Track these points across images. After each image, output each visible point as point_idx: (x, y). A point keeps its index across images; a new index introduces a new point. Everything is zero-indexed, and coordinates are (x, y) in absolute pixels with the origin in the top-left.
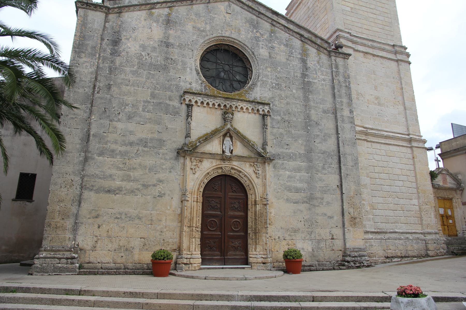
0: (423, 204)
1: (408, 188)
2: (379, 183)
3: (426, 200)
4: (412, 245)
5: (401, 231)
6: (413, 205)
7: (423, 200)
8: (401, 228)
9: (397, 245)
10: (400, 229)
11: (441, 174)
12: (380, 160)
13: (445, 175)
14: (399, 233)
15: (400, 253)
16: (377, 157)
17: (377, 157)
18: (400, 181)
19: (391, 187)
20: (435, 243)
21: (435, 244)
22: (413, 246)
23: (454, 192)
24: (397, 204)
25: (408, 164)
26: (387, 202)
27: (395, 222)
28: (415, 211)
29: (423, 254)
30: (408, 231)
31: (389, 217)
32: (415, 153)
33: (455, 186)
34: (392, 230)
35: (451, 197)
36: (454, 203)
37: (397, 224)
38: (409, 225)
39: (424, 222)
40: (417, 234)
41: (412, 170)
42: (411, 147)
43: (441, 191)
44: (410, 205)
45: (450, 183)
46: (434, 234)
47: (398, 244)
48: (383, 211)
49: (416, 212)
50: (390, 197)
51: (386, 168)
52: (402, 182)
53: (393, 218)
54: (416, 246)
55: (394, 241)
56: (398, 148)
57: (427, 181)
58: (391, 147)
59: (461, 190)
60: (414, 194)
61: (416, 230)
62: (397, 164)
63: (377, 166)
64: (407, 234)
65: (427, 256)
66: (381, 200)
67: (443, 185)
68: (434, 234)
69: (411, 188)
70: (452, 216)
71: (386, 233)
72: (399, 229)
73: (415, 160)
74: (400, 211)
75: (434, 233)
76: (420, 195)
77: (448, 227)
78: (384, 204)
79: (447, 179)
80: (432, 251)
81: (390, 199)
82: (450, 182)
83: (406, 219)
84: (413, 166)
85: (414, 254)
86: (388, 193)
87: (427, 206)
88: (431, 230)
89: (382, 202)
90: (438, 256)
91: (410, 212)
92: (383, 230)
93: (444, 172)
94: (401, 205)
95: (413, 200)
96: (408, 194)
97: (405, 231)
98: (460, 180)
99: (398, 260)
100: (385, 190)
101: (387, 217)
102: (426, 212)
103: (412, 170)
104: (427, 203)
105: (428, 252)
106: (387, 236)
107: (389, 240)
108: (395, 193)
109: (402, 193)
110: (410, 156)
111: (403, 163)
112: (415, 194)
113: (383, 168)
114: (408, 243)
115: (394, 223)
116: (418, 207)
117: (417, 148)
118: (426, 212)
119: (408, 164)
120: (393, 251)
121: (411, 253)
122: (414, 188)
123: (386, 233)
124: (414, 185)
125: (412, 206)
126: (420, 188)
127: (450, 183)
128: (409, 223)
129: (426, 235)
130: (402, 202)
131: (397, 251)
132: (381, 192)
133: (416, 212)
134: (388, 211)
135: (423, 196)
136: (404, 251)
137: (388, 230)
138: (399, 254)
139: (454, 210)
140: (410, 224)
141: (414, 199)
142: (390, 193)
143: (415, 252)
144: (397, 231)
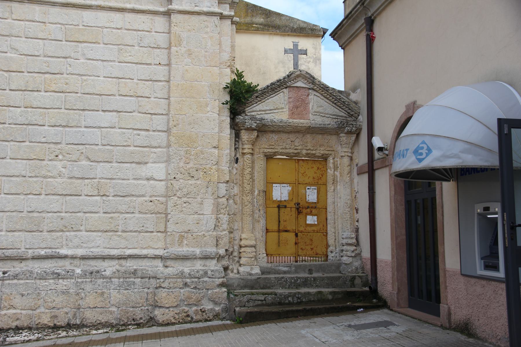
0: (178, 176)
1: (135, 132)
2: (21, 120)
3: (191, 165)
4: (103, 294)
5: (80, 252)
6: (148, 179)
7: (182, 164)
8: (85, 245)
9: (43, 293)
10: (82, 247)
11: (285, 90)
12: (36, 53)
13: (302, 90)
14: (73, 257)
15: (49, 315)
16: (23, 45)
17: (23, 45)
18: (107, 113)
19: (67, 129)
20: (186, 285)
21: (188, 289)
22: (105, 295)
23: (334, 137)
24: (82, 178)
25: (150, 64)
26: (44, 172)
27: (66, 227)
28: (151, 196)
29: (142, 315)
30: (107, 252)
31: (44, 215)
32: (174, 29)
33: (329, 122)
34: (43, 253)
35: (320, 151)
36: (329, 170)
37: (73, 233)
38: (119, 236)
39: (171, 227)
40: (146, 260)
41: (160, 81)
42: (168, 14)
43: (284, 136)
44: (135, 179)
45: (316, 114)
46: (200, 258)
47: (49, 292)
48: (22, 197)
49: (153, 199)
50: (60, 157)
51: (58, 76)
52: (115, 113)
53: (58, 217)
54: (116, 296)
55: (38, 281)
56: (117, 16)
57: (209, 109)
58: (87, 14)
59: (350, 133)
60: (155, 147)
61: (142, 248)
62: (105, 63)
63: (23, 70)
64: (106, 260)
65: (152, 321)
66: (20, 167)
67: (291, 120)
68: (200, 258)
69: (148, 130)
70: (319, 206)
71: (21, 259)
72: (77, 247)
73: (174, 49)
74: (88, 198)
75: (200, 256)
76: (170, 149)
77: (296, 235)
78: (31, 179)
79: (308, 103)
80: (168, 308)
81: (59, 165)
82: (320, 109)
83: (111, 218)
84: (166, 68)
85: (103, 319)
86: (52, 146)
87: (192, 182)
88: (192, 249)
89: (23, 173)
90: (190, 322)
91: (127, 199)
92: (8, 253)
93: (299, 84)
94: (97, 180)
95: (149, 165)
96: (132, 148)
97: (97, 251)
98: (356, 103)
99: (32, 337)
100: (44, 140)
101: (35, 215)
102: (185, 199)
103: (160, 81)
104: (194, 173)
105: (157, 312)
106: (18, 267)
107: (15, 281)
108: (81, 147)
109: (108, 147)
110: (162, 39)
111: (128, 59)
112: (159, 147)
113: (47, 76)
114: (88, 287)
115: (62, 231)
116: (163, 183)
117: (187, 16)
118: (185, 199)
119: (150, 64)
120: (23, 312)
121: (91, 316)
122: (159, 131)
123: (21, 259)
124: (160, 122)
125: (145, 182)
126: (174, 130)
127: (316, 114)
128: (120, 229)
129: (169, 263)
130: (101, 170)
131: (42, 309)
132: (27, 143)
133: (153, 199)
134: (43, 196)
135: (182, 153)
136: (66, 310)
137: (30, 251)
138: (46, 320)
139: (328, 189)
140: (124, 231)
141: (152, 163)
142: (59, 146)
143: (111, 313)
144: (63, 251)
